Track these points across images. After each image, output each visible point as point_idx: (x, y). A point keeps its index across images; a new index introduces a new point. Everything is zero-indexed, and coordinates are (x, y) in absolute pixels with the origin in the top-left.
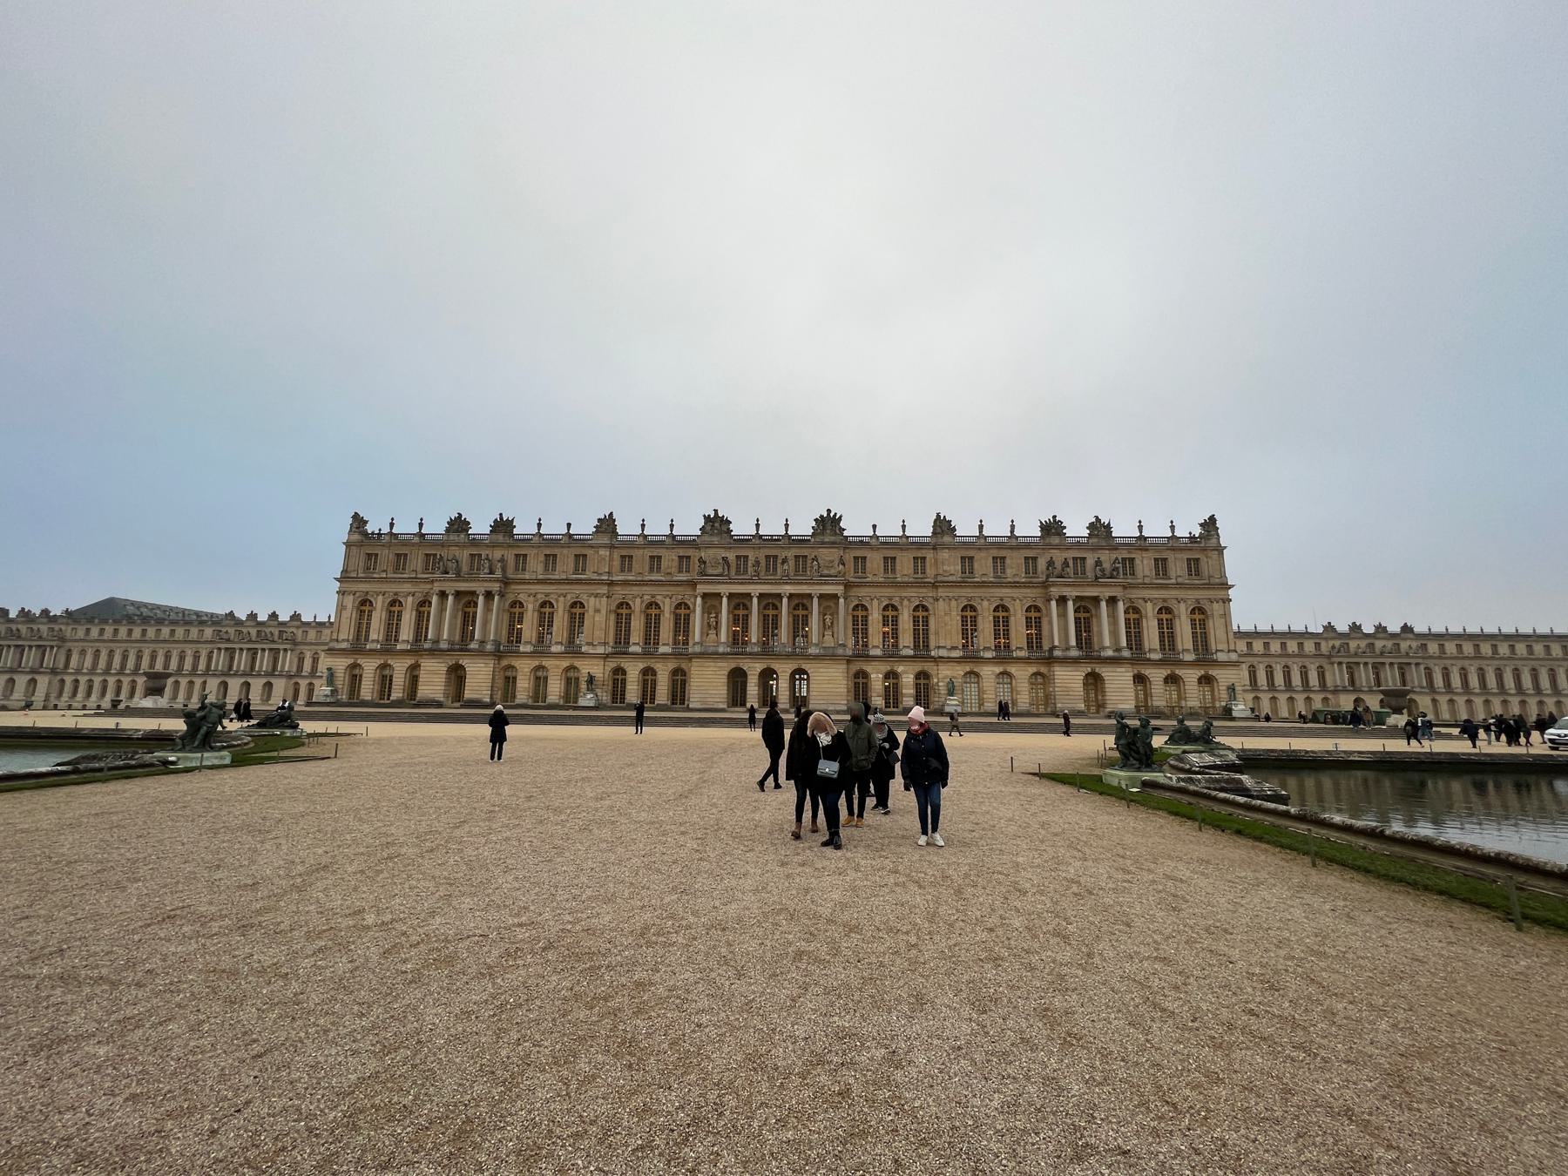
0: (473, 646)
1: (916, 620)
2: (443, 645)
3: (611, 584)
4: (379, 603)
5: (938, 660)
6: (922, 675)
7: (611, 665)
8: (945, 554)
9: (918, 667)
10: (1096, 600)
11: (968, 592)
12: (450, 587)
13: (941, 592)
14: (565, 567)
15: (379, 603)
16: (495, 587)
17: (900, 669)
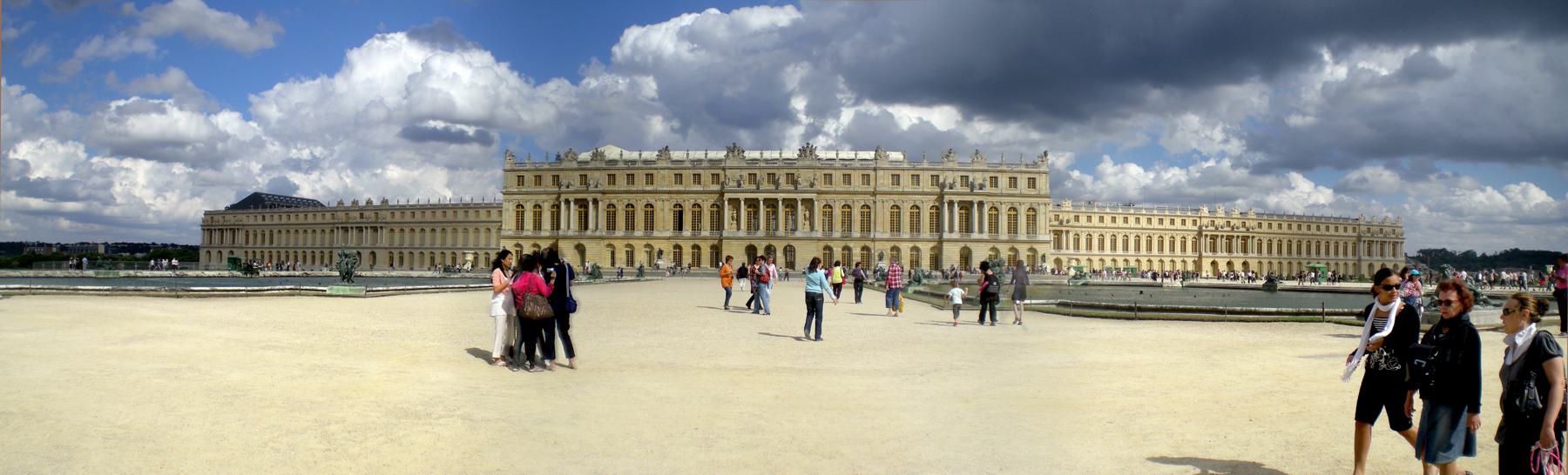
0: (589, 233)
1: (862, 214)
2: (571, 233)
3: (670, 192)
4: (529, 207)
5: (873, 240)
6: (865, 248)
7: (674, 242)
8: (880, 173)
9: (862, 244)
10: (971, 203)
11: (896, 197)
12: (571, 198)
13: (879, 197)
14: (641, 184)
15: (529, 207)
16: (599, 196)
17: (851, 245)
